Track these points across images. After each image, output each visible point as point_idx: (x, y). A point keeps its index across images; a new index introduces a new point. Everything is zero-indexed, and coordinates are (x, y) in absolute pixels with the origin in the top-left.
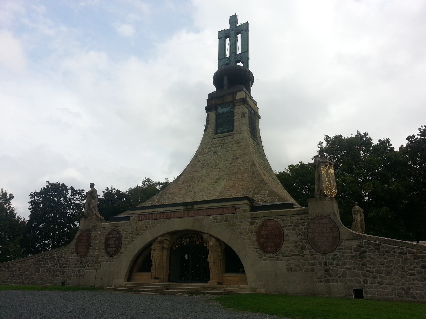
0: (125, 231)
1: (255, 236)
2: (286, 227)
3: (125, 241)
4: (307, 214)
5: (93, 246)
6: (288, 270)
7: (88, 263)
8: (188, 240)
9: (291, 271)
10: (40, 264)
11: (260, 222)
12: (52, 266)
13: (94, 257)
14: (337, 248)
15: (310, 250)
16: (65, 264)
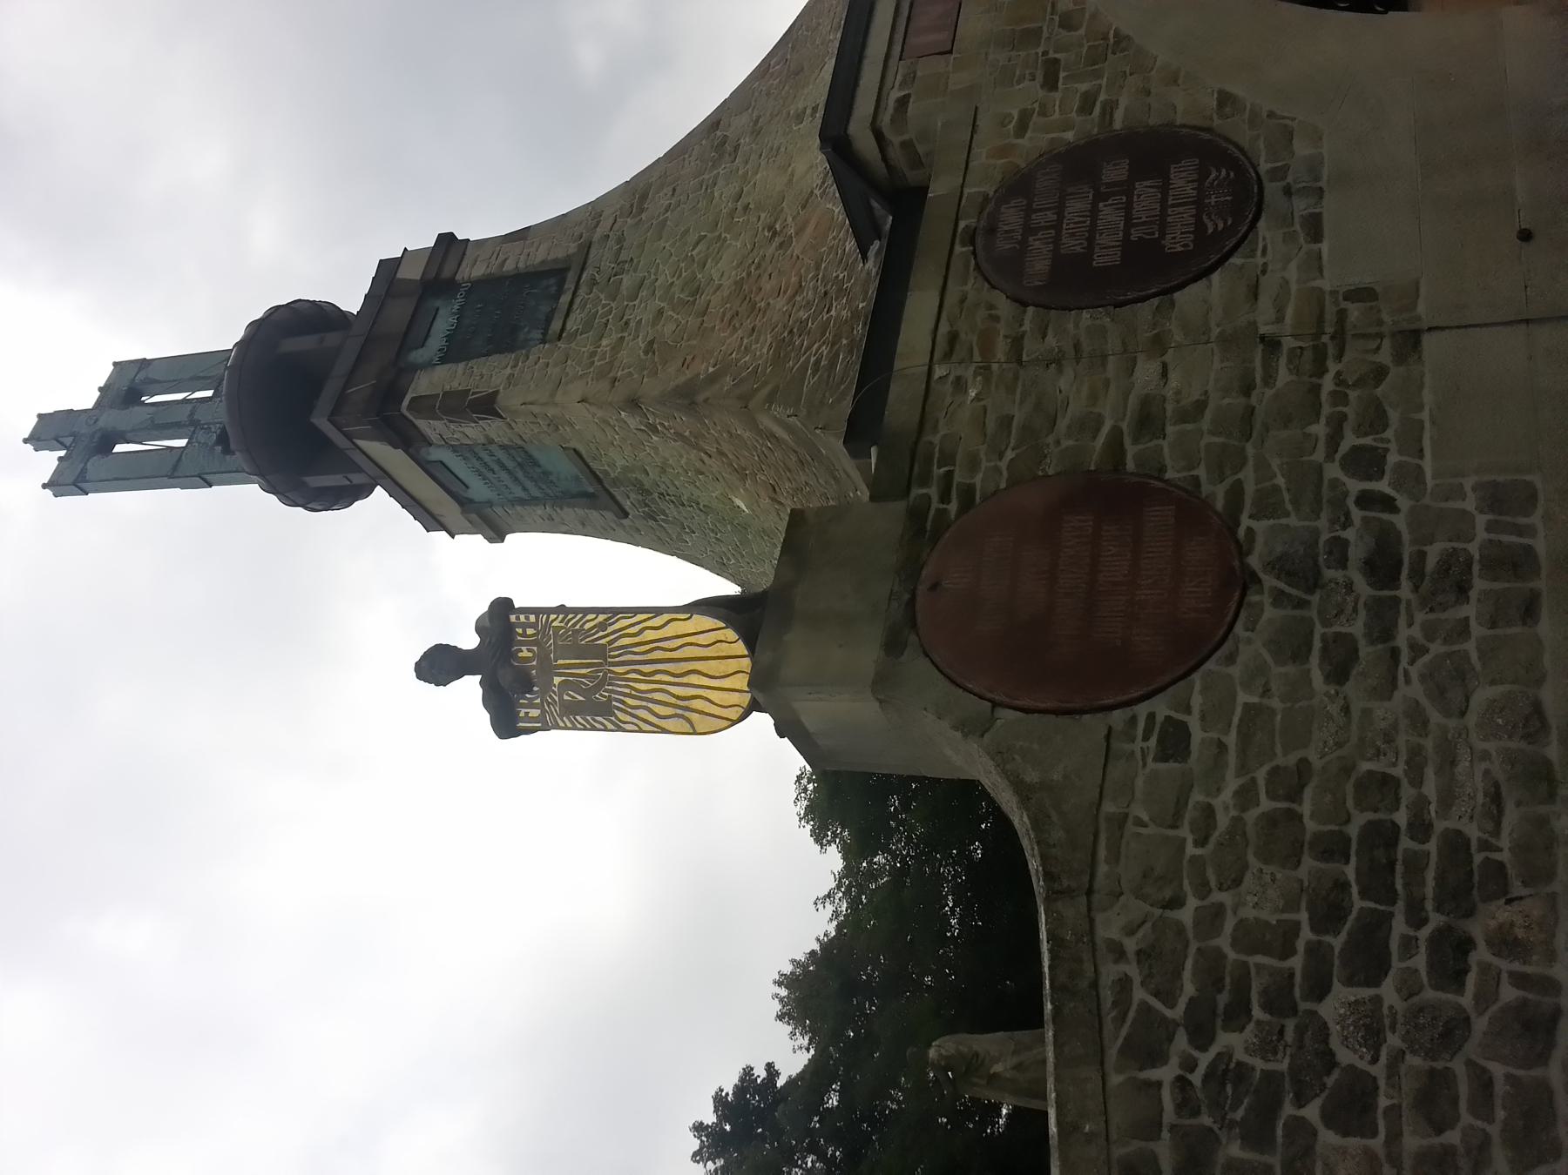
3: (1109, 108)
7: (1333, 471)
12: (1354, 1142)
13: (1247, 390)
16: (1331, 867)
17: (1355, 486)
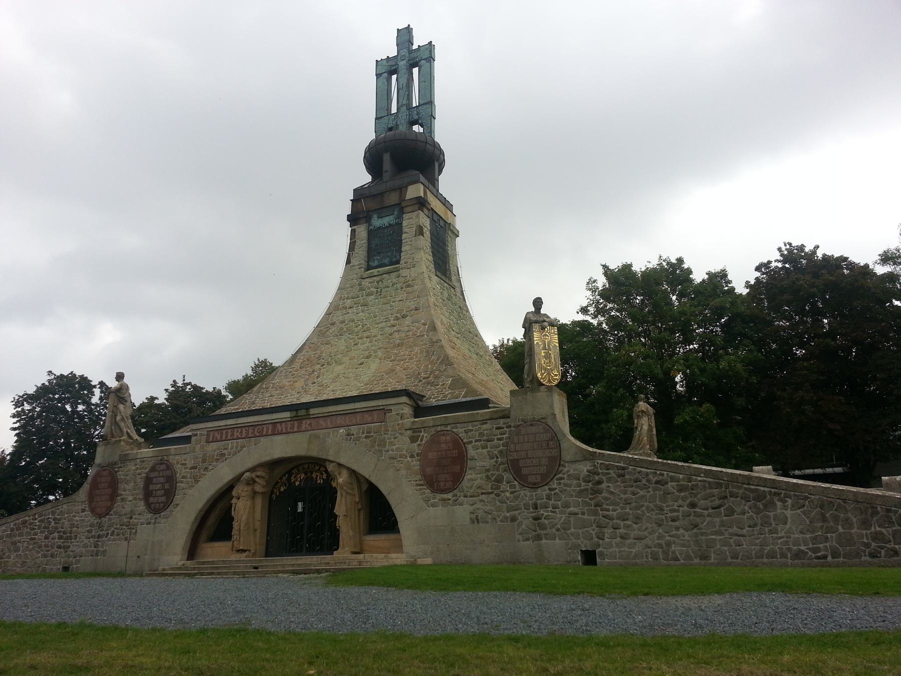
0: (182, 464)
1: (419, 462)
2: (473, 444)
3: (182, 482)
4: (509, 417)
5: (122, 495)
6: (473, 522)
7: (112, 529)
8: (303, 476)
9: (478, 523)
10: (21, 535)
11: (428, 436)
13: (125, 515)
14: (556, 477)
15: (510, 483)
17: (110, 532)
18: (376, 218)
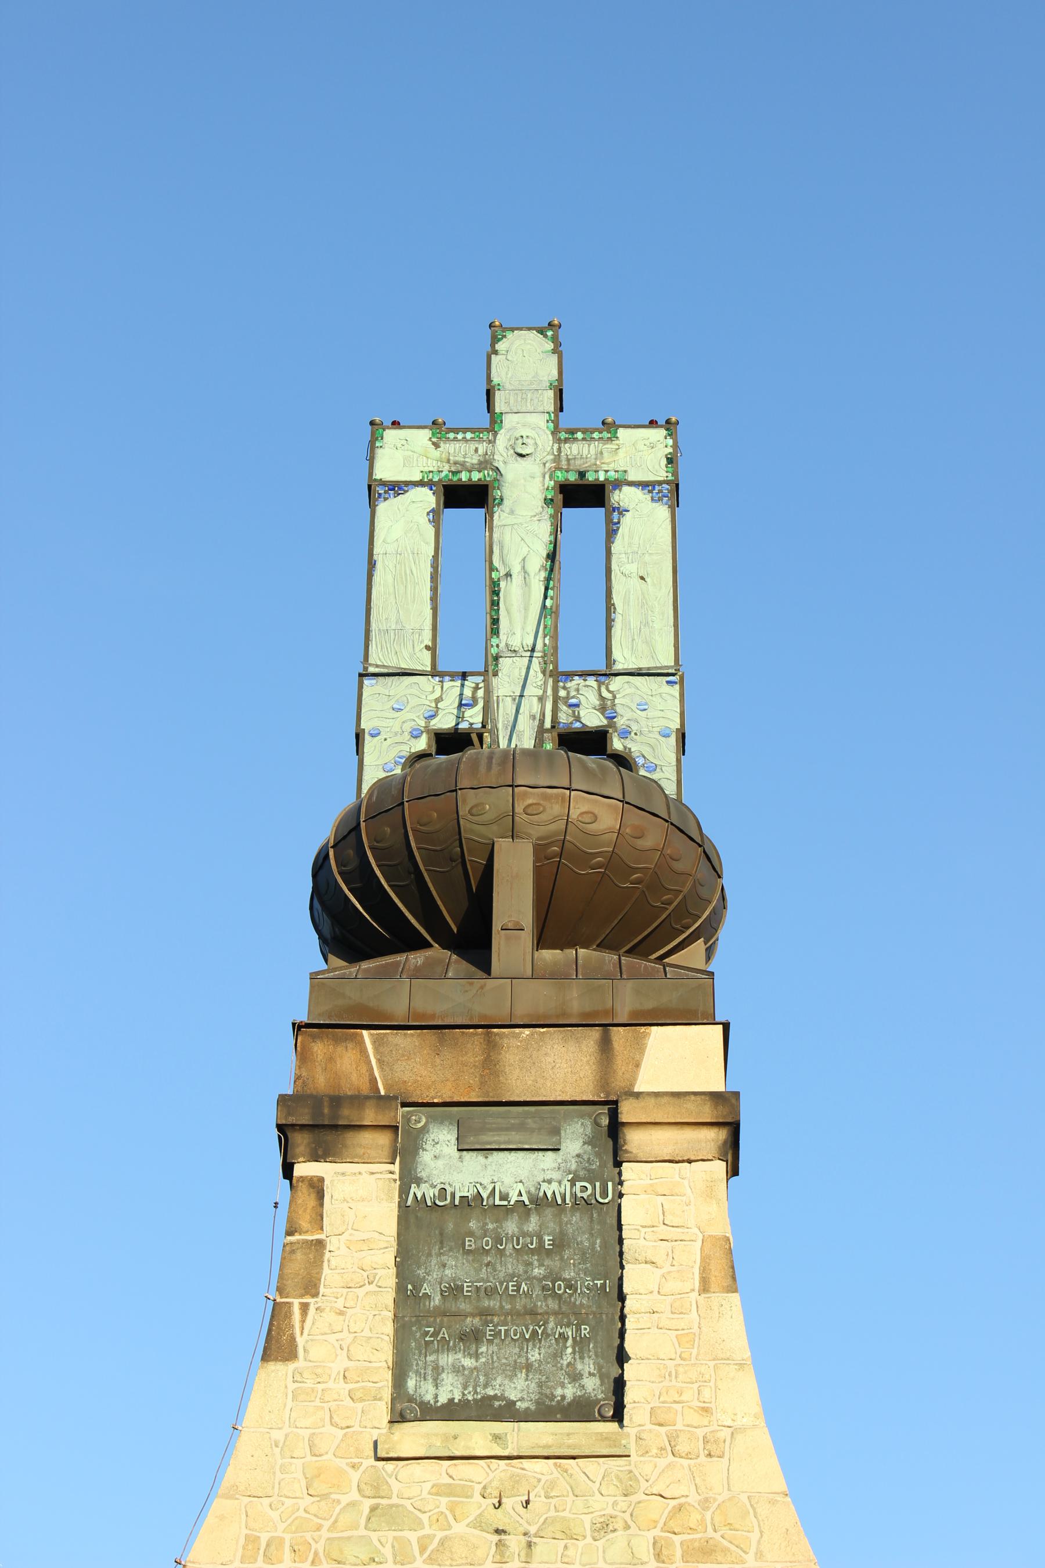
18: (452, 1150)
